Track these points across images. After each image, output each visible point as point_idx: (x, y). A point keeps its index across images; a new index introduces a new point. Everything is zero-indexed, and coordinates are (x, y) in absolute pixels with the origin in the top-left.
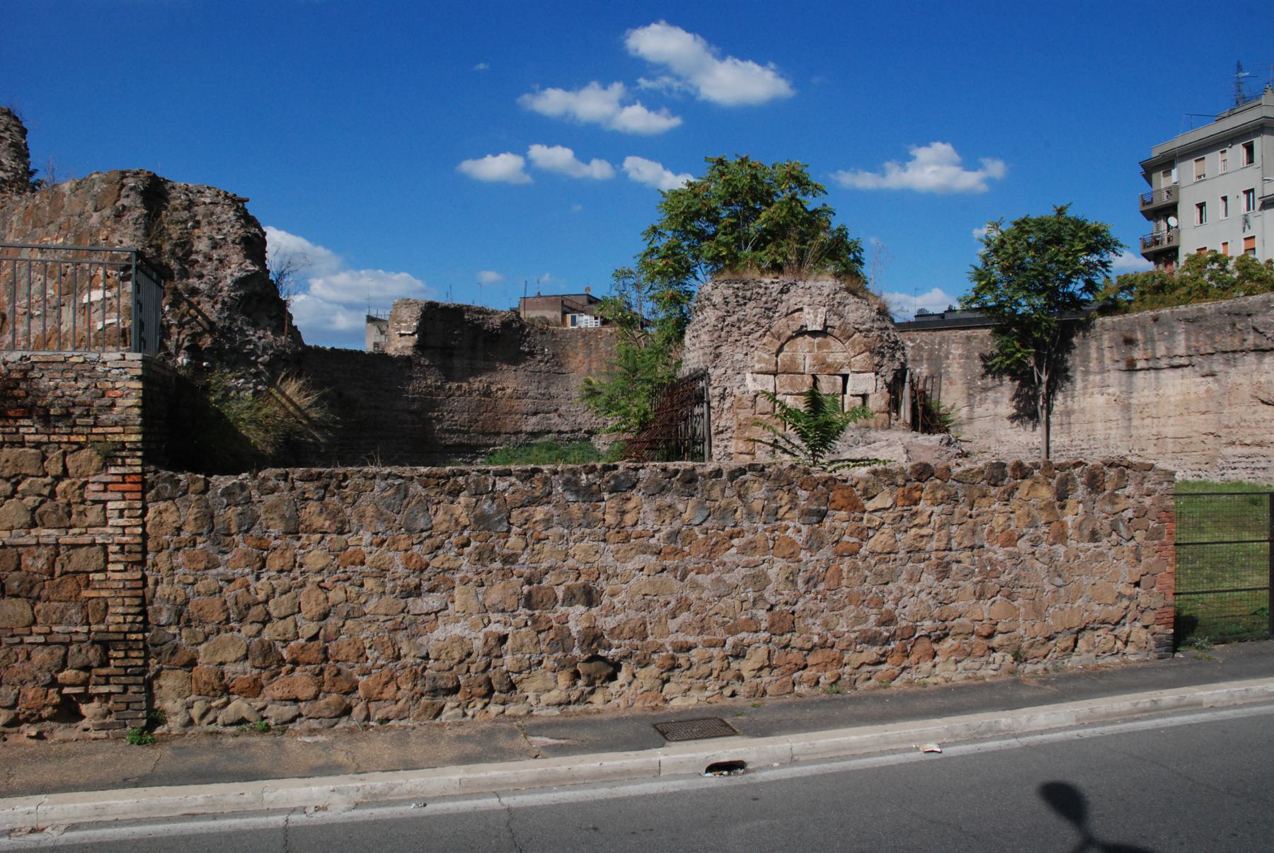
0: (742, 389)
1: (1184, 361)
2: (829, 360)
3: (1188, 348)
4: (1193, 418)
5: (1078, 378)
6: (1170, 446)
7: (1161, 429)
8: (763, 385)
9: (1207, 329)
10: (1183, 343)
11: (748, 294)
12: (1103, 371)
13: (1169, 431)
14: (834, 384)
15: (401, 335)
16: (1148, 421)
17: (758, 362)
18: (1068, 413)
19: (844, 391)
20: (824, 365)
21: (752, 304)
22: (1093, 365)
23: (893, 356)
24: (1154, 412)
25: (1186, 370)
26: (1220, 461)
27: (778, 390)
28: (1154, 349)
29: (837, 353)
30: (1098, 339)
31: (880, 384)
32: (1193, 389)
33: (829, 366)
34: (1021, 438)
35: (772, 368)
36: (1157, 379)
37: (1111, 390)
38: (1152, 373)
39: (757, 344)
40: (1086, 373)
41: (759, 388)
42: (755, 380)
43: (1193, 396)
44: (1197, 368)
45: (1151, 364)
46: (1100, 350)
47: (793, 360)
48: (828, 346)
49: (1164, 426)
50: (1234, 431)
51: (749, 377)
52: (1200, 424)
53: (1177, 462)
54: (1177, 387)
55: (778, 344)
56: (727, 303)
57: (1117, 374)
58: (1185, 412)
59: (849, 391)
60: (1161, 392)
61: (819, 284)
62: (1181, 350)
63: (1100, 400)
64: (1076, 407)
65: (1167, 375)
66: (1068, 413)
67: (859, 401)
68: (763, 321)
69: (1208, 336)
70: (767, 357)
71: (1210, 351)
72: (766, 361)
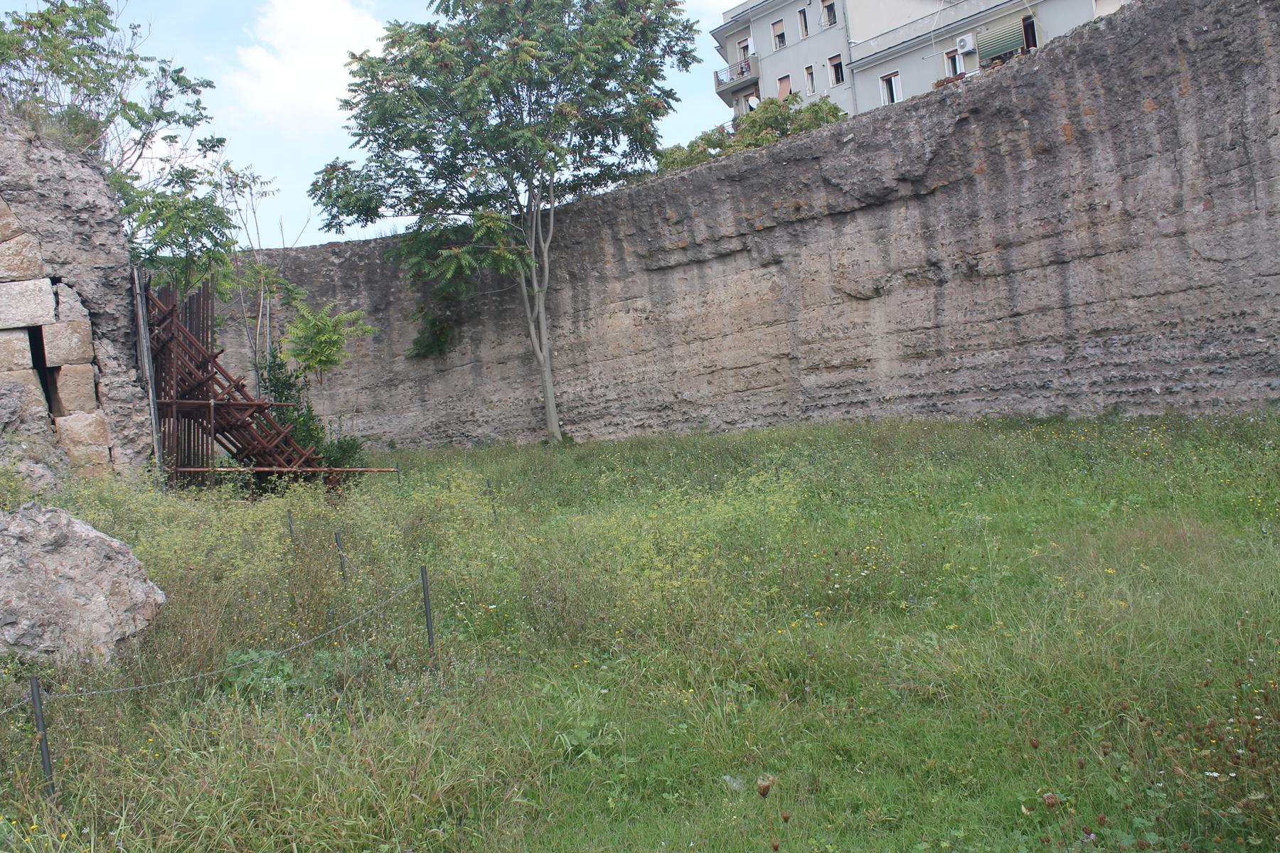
1: (735, 245)
3: (738, 222)
4: (757, 334)
5: (592, 284)
6: (731, 381)
7: (714, 356)
9: (763, 187)
10: (730, 217)
12: (624, 275)
13: (726, 359)
16: (696, 346)
18: (583, 346)
22: (611, 268)
23: (87, 239)
24: (703, 330)
25: (742, 261)
26: (801, 398)
28: (692, 232)
30: (612, 224)
31: (69, 299)
32: (753, 288)
34: (518, 393)
36: (701, 278)
37: (639, 303)
38: (695, 271)
40: (603, 279)
43: (753, 299)
44: (755, 255)
45: (691, 255)
46: (617, 241)
49: (718, 350)
50: (815, 346)
52: (769, 342)
53: (742, 406)
54: (735, 286)
57: (645, 277)
58: (745, 325)
60: (709, 298)
62: (728, 229)
63: (625, 321)
64: (592, 335)
65: (715, 271)
66: (583, 346)
67: (22, 342)
69: (763, 200)
71: (768, 224)
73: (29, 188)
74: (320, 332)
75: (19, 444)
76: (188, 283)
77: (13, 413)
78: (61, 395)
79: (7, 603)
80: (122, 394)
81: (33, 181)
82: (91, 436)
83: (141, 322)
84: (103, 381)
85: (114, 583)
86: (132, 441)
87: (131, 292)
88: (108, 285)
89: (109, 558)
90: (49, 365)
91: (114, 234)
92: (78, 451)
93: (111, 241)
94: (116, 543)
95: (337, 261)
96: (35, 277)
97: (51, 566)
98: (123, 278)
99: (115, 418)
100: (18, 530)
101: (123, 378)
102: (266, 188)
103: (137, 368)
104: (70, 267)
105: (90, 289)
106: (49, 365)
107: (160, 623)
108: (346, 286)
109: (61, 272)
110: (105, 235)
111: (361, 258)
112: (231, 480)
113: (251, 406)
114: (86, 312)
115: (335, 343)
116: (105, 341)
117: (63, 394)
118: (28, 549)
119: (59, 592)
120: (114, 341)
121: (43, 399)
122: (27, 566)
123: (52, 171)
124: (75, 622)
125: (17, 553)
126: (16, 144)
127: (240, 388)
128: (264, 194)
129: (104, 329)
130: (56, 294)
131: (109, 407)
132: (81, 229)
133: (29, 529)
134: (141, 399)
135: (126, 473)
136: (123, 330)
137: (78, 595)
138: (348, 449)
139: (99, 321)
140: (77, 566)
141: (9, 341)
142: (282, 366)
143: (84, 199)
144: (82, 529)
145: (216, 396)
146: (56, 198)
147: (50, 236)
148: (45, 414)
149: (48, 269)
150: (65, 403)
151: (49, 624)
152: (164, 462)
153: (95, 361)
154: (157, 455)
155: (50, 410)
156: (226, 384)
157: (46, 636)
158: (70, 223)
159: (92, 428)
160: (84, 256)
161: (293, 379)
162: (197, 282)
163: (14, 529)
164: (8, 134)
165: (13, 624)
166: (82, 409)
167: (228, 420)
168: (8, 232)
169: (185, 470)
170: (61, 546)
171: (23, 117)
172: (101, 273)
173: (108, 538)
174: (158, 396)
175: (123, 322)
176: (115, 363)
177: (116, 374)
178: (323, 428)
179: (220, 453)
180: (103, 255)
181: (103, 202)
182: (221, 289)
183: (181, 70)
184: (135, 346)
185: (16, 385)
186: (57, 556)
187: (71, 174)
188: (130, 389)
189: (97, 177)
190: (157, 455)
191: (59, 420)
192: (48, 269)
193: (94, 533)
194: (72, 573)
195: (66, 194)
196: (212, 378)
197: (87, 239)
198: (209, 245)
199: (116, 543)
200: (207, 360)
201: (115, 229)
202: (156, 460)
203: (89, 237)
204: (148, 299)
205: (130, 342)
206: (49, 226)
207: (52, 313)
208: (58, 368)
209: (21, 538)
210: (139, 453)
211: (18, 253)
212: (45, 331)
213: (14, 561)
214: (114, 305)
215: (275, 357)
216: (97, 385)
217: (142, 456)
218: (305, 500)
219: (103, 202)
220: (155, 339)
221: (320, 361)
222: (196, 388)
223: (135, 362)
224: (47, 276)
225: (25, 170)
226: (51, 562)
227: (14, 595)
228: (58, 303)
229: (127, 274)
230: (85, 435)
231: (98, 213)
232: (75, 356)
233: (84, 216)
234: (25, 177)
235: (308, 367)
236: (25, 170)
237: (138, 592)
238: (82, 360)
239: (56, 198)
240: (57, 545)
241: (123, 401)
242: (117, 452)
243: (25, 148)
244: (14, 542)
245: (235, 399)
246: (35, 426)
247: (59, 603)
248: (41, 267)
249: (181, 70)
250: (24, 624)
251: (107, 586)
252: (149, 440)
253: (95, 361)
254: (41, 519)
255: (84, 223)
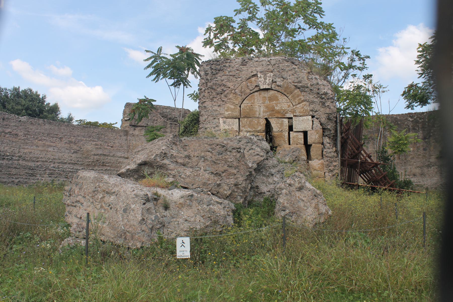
0: (217, 128)
2: (277, 108)
8: (229, 125)
11: (218, 67)
14: (282, 124)
15: (126, 120)
17: (227, 111)
19: (291, 128)
20: (273, 112)
21: (221, 73)
23: (323, 104)
27: (241, 128)
29: (283, 104)
31: (317, 123)
33: (278, 112)
35: (237, 114)
39: (225, 99)
41: (227, 127)
42: (224, 122)
47: (251, 109)
48: (276, 99)
51: (221, 121)
55: (240, 99)
56: (207, 74)
59: (294, 130)
61: (269, 59)
67: (301, 136)
68: (229, 84)
70: (233, 107)
72: (232, 110)
73: (307, 87)
74: (400, 140)
75: (297, 167)
76: (355, 121)
77: (296, 157)
78: (311, 154)
79: (284, 204)
80: (330, 155)
81: (309, 85)
82: (319, 168)
83: (338, 132)
84: (325, 150)
85: (316, 204)
86: (332, 171)
87: (336, 122)
88: (329, 119)
89: (316, 196)
90: (308, 144)
91: (332, 102)
92: (314, 172)
93: (331, 104)
94: (318, 192)
95: (411, 120)
96: (307, 115)
97: (297, 195)
98: (334, 117)
99: (327, 163)
100: (289, 182)
101: (331, 150)
102: (384, 90)
103: (336, 147)
104: (317, 113)
105: (323, 120)
106: (308, 144)
107: (329, 220)
108: (414, 129)
109: (315, 114)
110: (329, 102)
111: (420, 119)
112: (363, 187)
113: (373, 164)
114: (321, 127)
115: (405, 144)
116: (327, 137)
117: (312, 153)
118: (291, 188)
119: (299, 204)
120: (329, 138)
121: (305, 154)
122: (290, 194)
123: (314, 82)
124: (302, 214)
125: (288, 189)
126: (305, 74)
127: (370, 157)
128: (384, 92)
129: (326, 133)
130: (313, 121)
131: (326, 159)
132: (322, 100)
133: (292, 182)
134: (336, 157)
135: (329, 181)
136: (332, 134)
137: (305, 206)
138: (407, 184)
139: (325, 131)
140: (305, 197)
141: (297, 135)
142: (386, 152)
143: (324, 91)
144: (308, 185)
145: (361, 159)
146: (315, 90)
147: (313, 102)
148: (306, 159)
149: (311, 113)
150: (312, 157)
151: (295, 213)
152: (341, 179)
153: (323, 144)
154: (339, 176)
155: (308, 158)
156: (365, 155)
157: (293, 217)
158: (319, 98)
159: (319, 165)
160: (322, 109)
161: (389, 157)
162: (358, 121)
163: (288, 182)
164: (303, 71)
165: (284, 210)
166: (317, 159)
167: (365, 168)
168: (300, 101)
169: (349, 184)
170: (301, 189)
171: (308, 66)
172: (327, 115)
173: (316, 190)
174: (342, 156)
175: (333, 132)
176: (329, 145)
177: (329, 148)
178: (399, 175)
179: (361, 181)
180: (328, 109)
181: (330, 92)
182: (367, 124)
183: (359, 51)
184: (336, 140)
185: (298, 149)
186: (300, 192)
187: (320, 83)
188: (333, 154)
189: (328, 84)
190: (339, 176)
191: (310, 162)
192: (311, 113)
193: (312, 187)
194: (303, 199)
195: (318, 89)
196: (360, 152)
197: (323, 104)
198: (363, 108)
199: (318, 192)
200: (359, 147)
201: (333, 101)
202: (339, 178)
203: (324, 103)
204: (341, 125)
205: (334, 138)
206: (312, 99)
207: (311, 127)
208: (311, 145)
209: (290, 185)
210: (334, 175)
211: (303, 108)
212: (309, 133)
213: (287, 192)
214: (330, 126)
215: (384, 149)
216: (322, 151)
217: (335, 177)
218: (388, 198)
219: (330, 92)
220: (342, 138)
221: (399, 150)
222: (356, 156)
223: (335, 145)
224: (311, 115)
225: (307, 82)
226: (298, 194)
227: (286, 202)
228: (313, 124)
229: (335, 116)
230: (317, 168)
231: (328, 95)
232: (317, 141)
233: (323, 96)
234: (307, 84)
235: (395, 153)
236: (307, 82)
237: (323, 209)
238: (319, 143)
239: (315, 90)
240: (300, 189)
241: (330, 157)
242: (327, 174)
243: (307, 75)
244: (288, 185)
245: (367, 161)
246: (302, 163)
247: (298, 207)
248: (309, 112)
249: (359, 51)
250: (287, 211)
251: (313, 205)
252: (336, 171)
253: (323, 144)
254: (296, 180)
255: (323, 98)
